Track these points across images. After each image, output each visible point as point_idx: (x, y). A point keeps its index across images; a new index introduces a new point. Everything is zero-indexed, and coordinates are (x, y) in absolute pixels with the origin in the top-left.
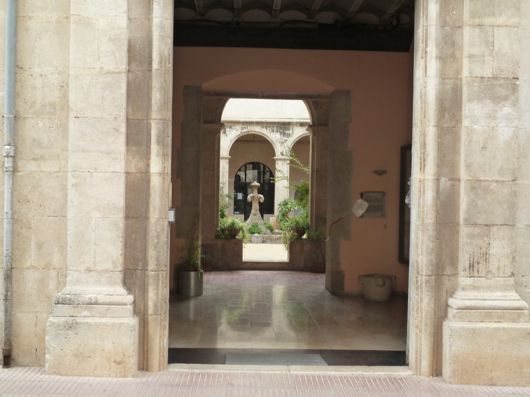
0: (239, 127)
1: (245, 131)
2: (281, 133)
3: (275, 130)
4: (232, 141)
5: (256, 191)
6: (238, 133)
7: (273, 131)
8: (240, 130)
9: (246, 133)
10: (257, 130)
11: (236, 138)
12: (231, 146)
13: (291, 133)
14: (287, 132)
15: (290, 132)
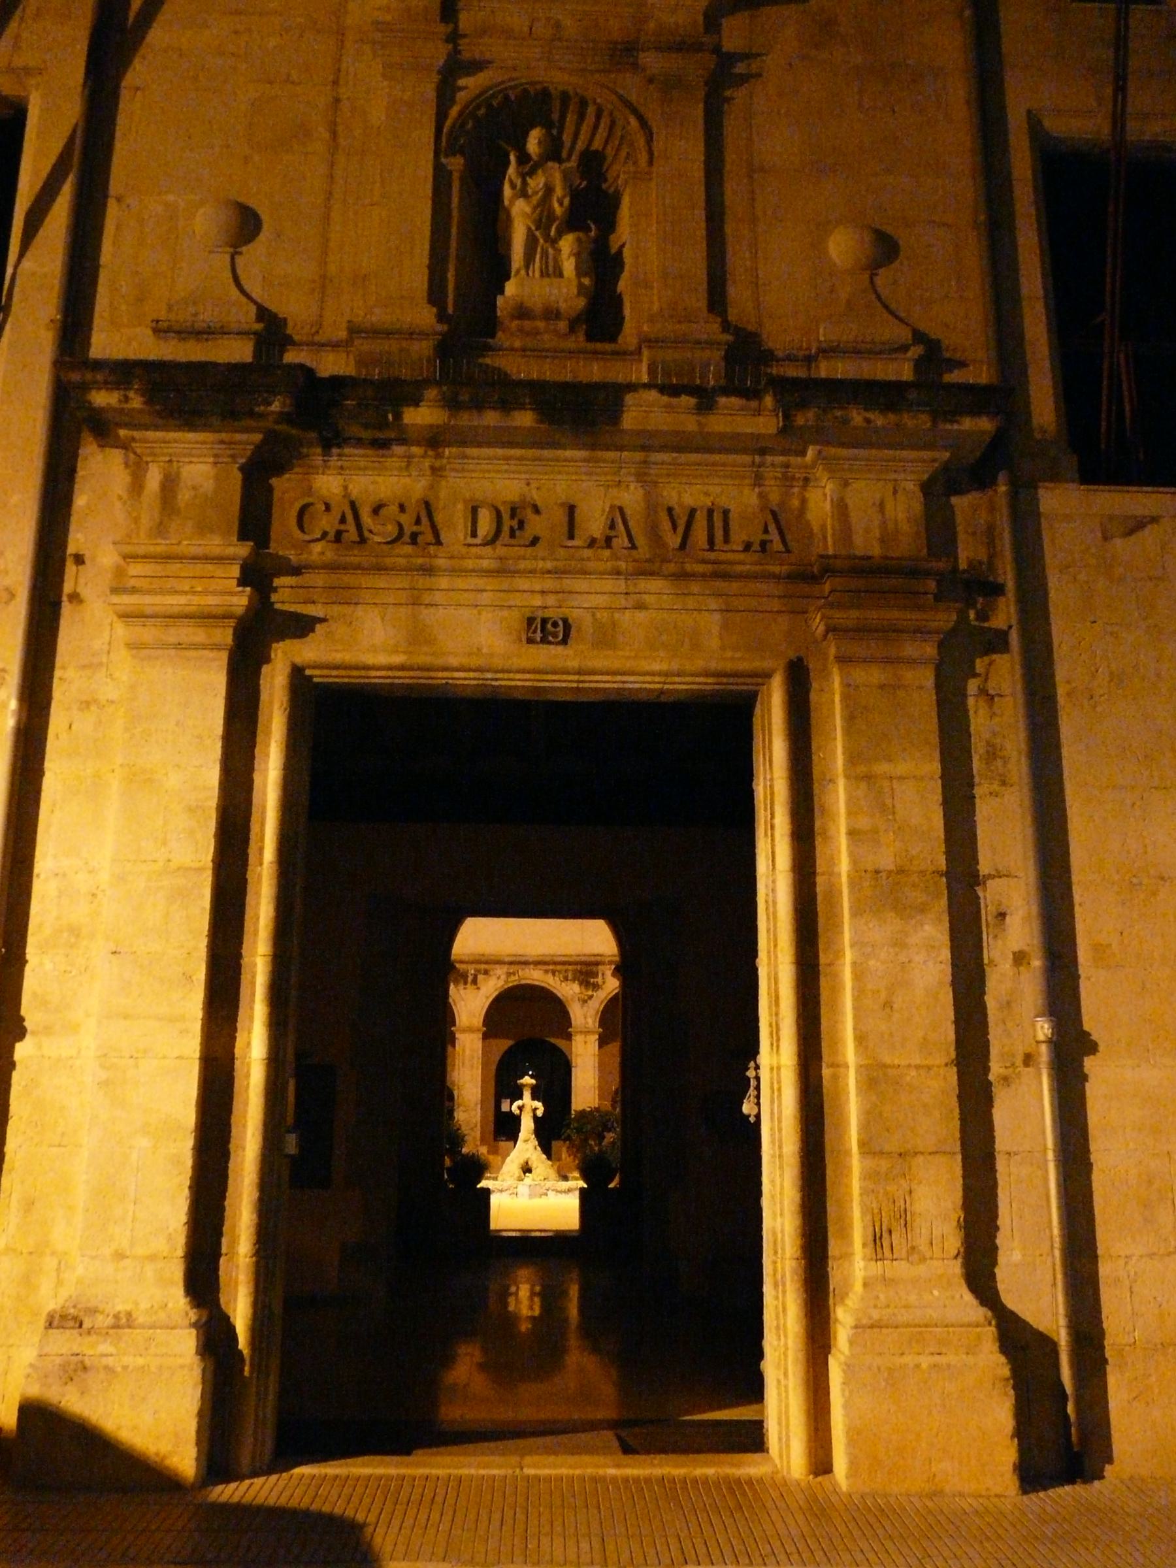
0: (501, 971)
2: (581, 984)
3: (570, 977)
5: (527, 1095)
6: (501, 983)
7: (566, 979)
8: (503, 977)
12: (487, 1006)
15: (599, 980)
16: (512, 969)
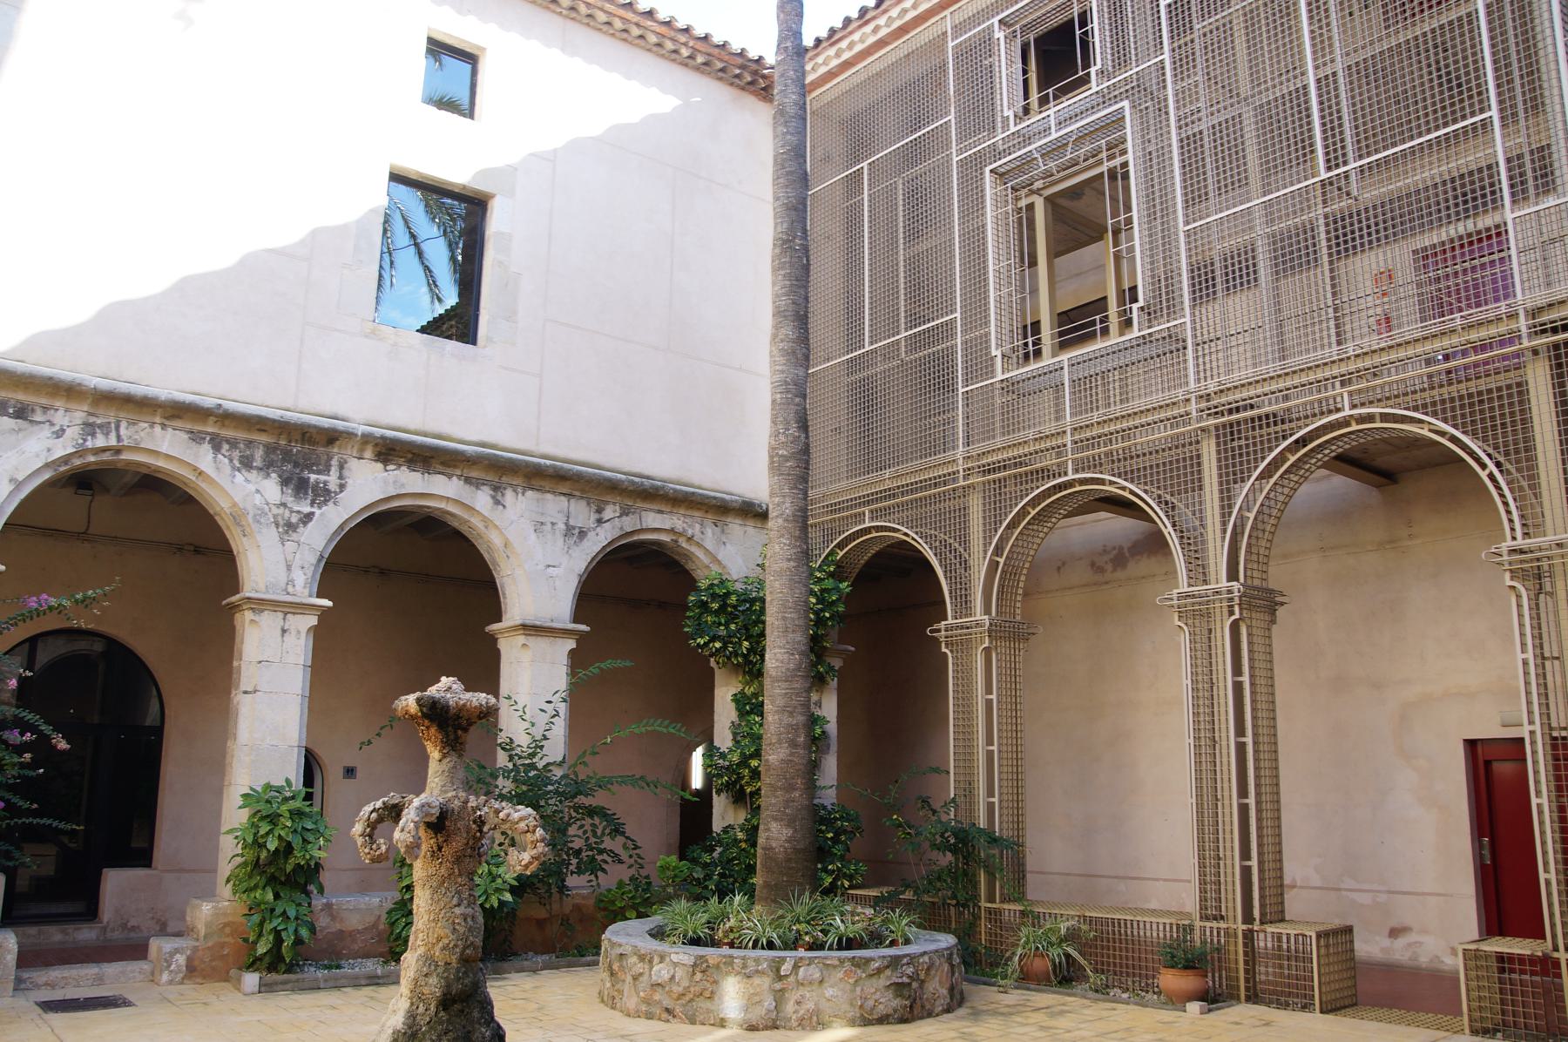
0: (70, 418)
1: (100, 441)
2: (285, 482)
3: (258, 462)
4: (19, 485)
6: (62, 448)
7: (247, 463)
8: (73, 433)
9: (106, 457)
10: (164, 448)
11: (47, 476)
13: (333, 487)
14: (313, 477)
16: (106, 416)
